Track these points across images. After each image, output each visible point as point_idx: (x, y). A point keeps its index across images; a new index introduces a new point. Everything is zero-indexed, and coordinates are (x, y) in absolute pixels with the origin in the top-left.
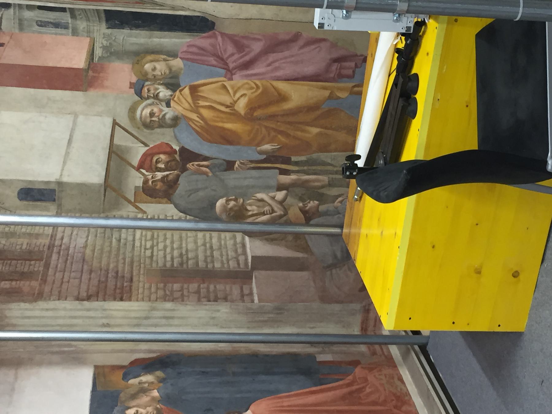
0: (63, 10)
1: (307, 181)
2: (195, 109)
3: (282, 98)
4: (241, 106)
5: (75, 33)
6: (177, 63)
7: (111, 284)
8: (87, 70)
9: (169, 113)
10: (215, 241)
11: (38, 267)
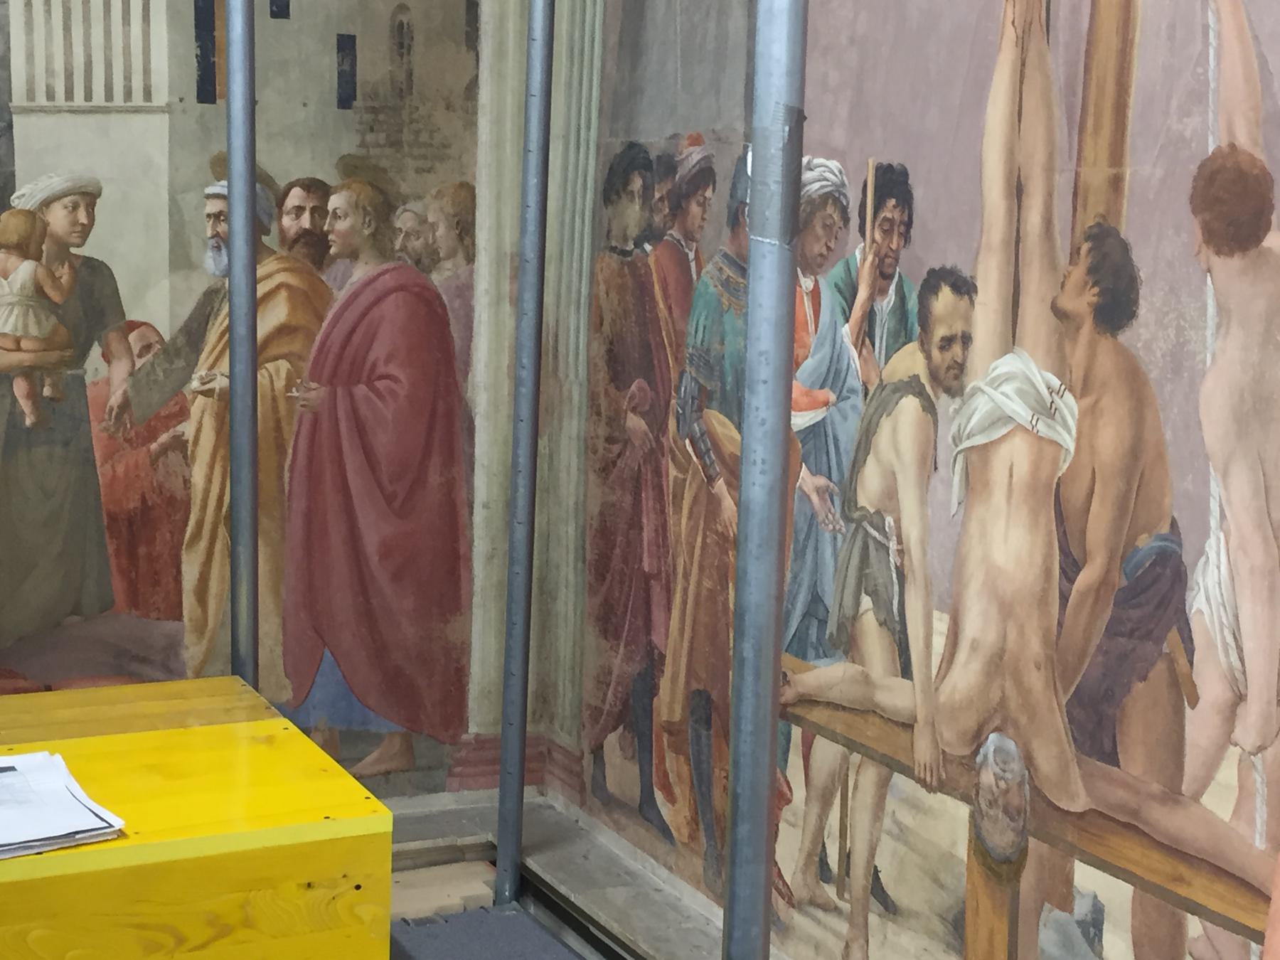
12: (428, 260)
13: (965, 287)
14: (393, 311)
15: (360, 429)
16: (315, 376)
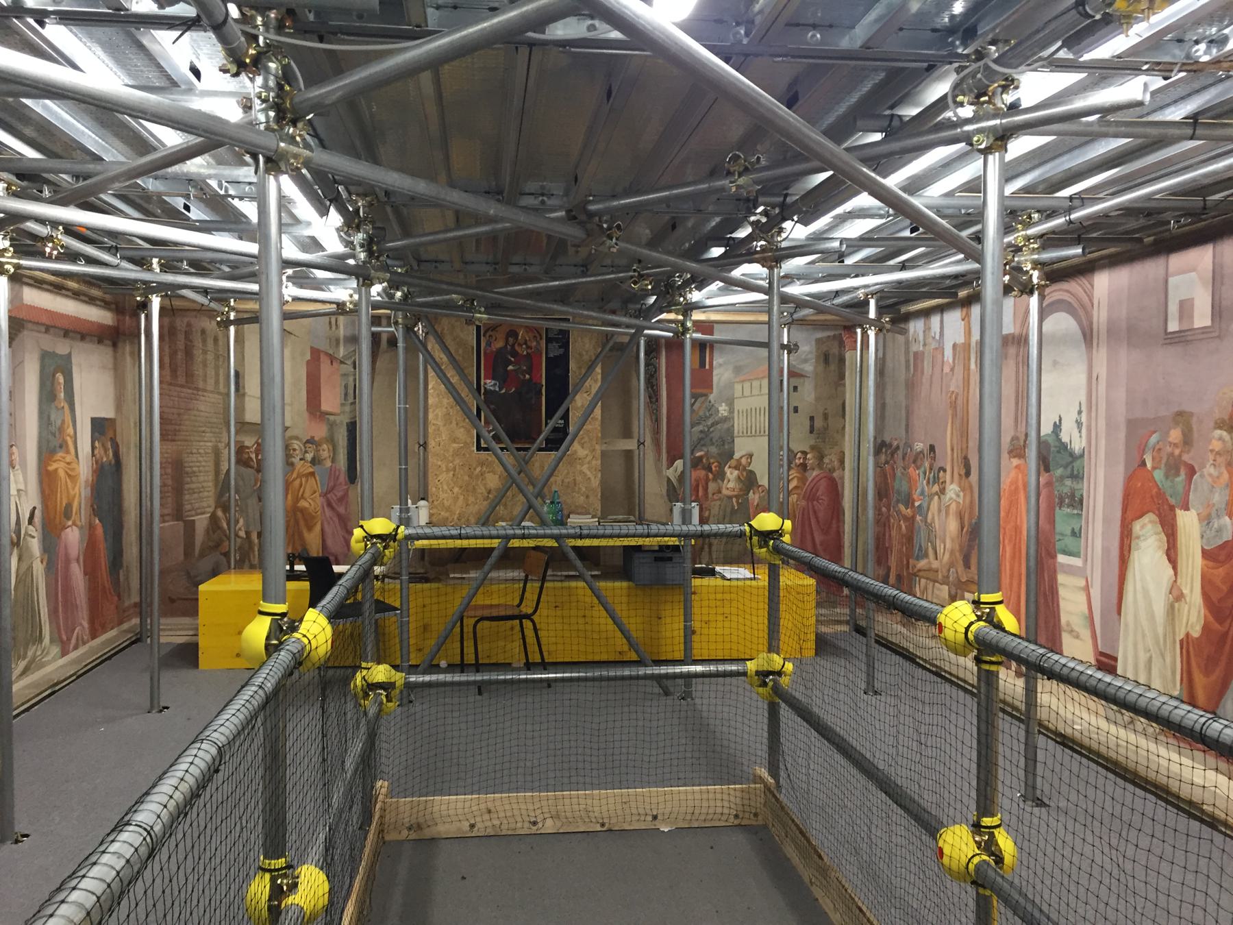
0: (355, 398)
1: (254, 551)
2: (300, 476)
3: (310, 528)
4: (303, 504)
5: (342, 405)
6: (328, 464)
7: (169, 427)
8: (320, 411)
9: (296, 460)
10: (206, 494)
11: (181, 380)
12: (832, 470)
13: (945, 471)
14: (823, 485)
15: (815, 512)
16: (804, 497)
